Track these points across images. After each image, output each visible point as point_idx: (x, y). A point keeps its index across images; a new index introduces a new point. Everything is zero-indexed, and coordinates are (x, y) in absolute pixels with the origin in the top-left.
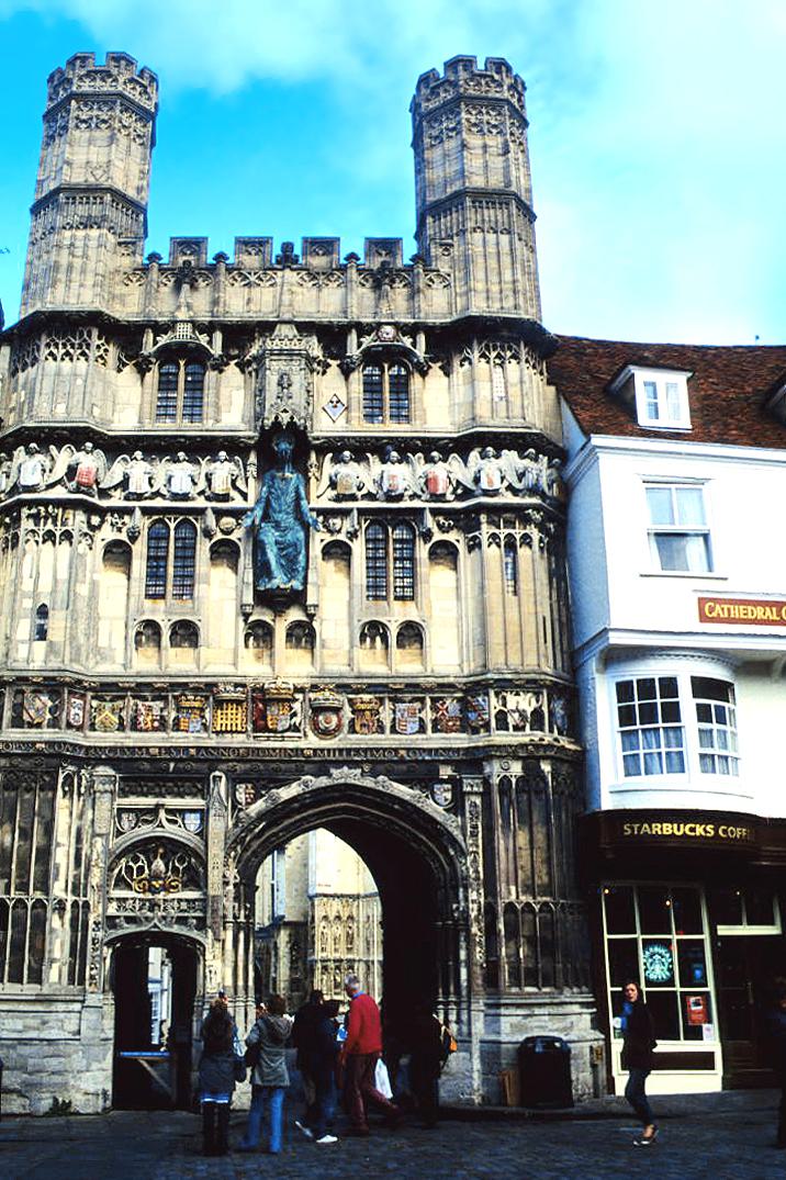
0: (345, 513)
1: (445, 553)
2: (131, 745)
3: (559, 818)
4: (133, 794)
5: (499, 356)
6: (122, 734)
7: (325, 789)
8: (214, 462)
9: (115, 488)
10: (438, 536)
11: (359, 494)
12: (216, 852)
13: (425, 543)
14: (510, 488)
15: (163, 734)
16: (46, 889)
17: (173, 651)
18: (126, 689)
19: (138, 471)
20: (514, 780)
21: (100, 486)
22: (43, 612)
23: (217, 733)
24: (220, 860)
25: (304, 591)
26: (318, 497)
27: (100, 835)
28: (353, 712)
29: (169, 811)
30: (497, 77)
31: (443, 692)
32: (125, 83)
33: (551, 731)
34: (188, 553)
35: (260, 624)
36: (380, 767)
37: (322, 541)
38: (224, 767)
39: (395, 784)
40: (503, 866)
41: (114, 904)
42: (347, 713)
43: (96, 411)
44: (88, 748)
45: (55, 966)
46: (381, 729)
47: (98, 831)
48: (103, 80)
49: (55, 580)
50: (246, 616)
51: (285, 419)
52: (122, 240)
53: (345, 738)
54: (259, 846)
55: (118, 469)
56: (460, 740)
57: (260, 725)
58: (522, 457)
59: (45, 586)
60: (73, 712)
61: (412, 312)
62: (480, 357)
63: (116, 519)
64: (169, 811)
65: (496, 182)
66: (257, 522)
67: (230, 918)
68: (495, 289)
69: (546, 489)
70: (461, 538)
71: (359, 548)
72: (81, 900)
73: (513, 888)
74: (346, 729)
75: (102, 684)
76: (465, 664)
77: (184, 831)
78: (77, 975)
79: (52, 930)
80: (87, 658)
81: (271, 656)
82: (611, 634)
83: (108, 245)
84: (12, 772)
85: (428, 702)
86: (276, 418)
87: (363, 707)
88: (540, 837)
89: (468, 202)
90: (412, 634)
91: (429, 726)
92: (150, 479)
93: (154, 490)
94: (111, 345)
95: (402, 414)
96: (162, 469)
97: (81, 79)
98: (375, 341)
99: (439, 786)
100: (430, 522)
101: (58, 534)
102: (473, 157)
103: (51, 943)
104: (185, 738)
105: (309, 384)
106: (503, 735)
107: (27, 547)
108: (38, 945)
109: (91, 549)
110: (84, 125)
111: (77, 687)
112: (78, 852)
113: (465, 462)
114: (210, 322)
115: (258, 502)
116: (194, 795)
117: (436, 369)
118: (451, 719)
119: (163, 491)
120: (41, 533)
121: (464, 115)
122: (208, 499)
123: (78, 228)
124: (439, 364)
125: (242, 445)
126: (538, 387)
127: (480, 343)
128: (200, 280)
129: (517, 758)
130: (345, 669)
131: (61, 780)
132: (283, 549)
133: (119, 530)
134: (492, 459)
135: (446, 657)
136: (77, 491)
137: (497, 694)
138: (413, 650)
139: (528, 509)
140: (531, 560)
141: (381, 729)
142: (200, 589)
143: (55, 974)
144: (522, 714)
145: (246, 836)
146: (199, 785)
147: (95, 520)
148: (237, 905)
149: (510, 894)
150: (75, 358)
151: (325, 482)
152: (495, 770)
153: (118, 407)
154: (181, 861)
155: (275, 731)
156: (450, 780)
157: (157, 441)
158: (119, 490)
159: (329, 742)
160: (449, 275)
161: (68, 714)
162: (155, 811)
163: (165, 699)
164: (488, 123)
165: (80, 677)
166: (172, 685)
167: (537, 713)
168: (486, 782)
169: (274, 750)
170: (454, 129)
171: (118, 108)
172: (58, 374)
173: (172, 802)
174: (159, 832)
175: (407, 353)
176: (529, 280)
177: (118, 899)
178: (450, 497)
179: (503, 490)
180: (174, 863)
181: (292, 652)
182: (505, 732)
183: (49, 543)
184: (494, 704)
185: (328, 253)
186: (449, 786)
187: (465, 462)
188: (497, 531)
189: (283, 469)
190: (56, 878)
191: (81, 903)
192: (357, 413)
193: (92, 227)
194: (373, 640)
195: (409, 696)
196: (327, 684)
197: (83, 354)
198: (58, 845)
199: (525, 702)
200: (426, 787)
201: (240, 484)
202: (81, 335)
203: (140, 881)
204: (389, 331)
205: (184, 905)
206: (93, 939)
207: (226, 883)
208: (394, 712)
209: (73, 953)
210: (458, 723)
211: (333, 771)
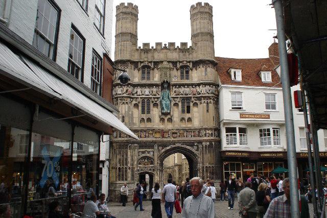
1: (195, 104)
10: (195, 102)
12: (156, 158)
16: (127, 165)
19: (139, 90)
22: (123, 117)
35: (162, 118)
46: (184, 136)
71: (180, 104)
77: (150, 155)
78: (133, 178)
88: (212, 156)
90: (190, 120)
95: (187, 78)
97: (122, 8)
112: (132, 159)
117: (194, 69)
135: (196, 123)
140: (211, 106)
141: (184, 136)
146: (152, 147)
147: (132, 100)
149: (207, 165)
152: (204, 144)
162: (145, 152)
167: (212, 134)
173: (148, 150)
175: (189, 66)
199: (210, 132)
204: (185, 62)
209: (132, 176)
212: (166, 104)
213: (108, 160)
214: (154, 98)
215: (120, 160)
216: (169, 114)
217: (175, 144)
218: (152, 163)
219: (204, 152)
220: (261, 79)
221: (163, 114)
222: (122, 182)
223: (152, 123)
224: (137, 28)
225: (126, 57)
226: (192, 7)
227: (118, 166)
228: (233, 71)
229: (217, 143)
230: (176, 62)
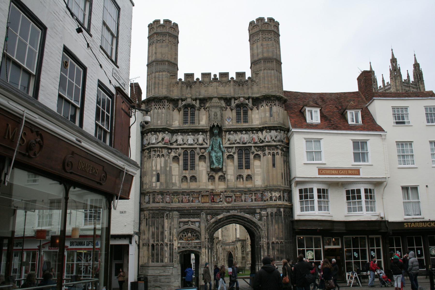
0: (232, 147)
1: (257, 157)
3: (285, 221)
4: (183, 218)
5: (271, 105)
6: (179, 204)
7: (229, 216)
8: (199, 135)
9: (174, 142)
10: (256, 153)
11: (236, 142)
12: (203, 232)
13: (253, 154)
16: (163, 240)
17: (191, 183)
18: (179, 193)
19: (179, 138)
20: (274, 213)
21: (171, 142)
23: (202, 203)
24: (204, 233)
25: (222, 168)
28: (235, 197)
30: (270, 23)
33: (283, 200)
34: (193, 158)
36: (242, 210)
38: (204, 211)
39: (246, 214)
40: (271, 233)
41: (179, 244)
42: (234, 198)
43: (168, 122)
44: (171, 208)
45: (166, 259)
46: (242, 201)
47: (175, 227)
49: (161, 167)
50: (208, 174)
51: (216, 124)
52: (171, 75)
55: (175, 138)
56: (261, 203)
57: (213, 201)
58: (276, 132)
59: (159, 168)
63: (175, 150)
64: (191, 222)
66: (210, 151)
67: (207, 247)
69: (283, 140)
70: (262, 153)
71: (236, 156)
73: (274, 238)
74: (233, 201)
75: (174, 192)
77: (195, 227)
78: (171, 260)
79: (165, 250)
81: (215, 184)
82: (296, 178)
86: (214, 124)
87: (237, 196)
90: (249, 177)
91: (254, 200)
92: (183, 140)
93: (184, 143)
95: (246, 121)
97: (157, 28)
101: (161, 155)
103: (165, 253)
107: (153, 158)
108: (162, 254)
110: (159, 42)
111: (168, 193)
113: (262, 133)
114: (196, 98)
115: (210, 145)
116: (197, 218)
118: (259, 198)
119: (186, 143)
120: (156, 155)
121: (261, 36)
122: (198, 145)
123: (159, 72)
124: (256, 107)
126: (282, 112)
127: (266, 101)
128: (193, 85)
129: (275, 207)
132: (217, 157)
133: (176, 153)
136: (165, 144)
137: (270, 192)
138: (249, 182)
140: (279, 159)
141: (242, 201)
142: (197, 168)
143: (166, 260)
144: (276, 197)
147: (170, 151)
151: (227, 140)
152: (269, 210)
154: (195, 233)
155: (216, 202)
156: (260, 213)
157: (184, 130)
161: (166, 200)
162: (188, 222)
163: (189, 195)
164: (268, 38)
165: (169, 191)
166: (191, 192)
167: (280, 196)
168: (267, 213)
169: (216, 207)
170: (258, 39)
171: (167, 36)
172: (158, 112)
173: (192, 220)
174: (189, 227)
175: (247, 105)
176: (279, 82)
177: (180, 243)
178: (259, 143)
179: (271, 141)
181: (220, 183)
183: (159, 157)
184: (270, 195)
187: (262, 133)
189: (216, 137)
190: (166, 238)
192: (235, 121)
194: (240, 179)
195: (249, 193)
197: (164, 107)
198: (166, 231)
199: (277, 194)
201: (206, 141)
202: (163, 102)
205: (196, 244)
207: (206, 238)
211: (231, 212)
212: (216, 157)
213: (136, 233)
214: (201, 149)
215: (153, 234)
216: (221, 170)
217: (229, 212)
218: (198, 238)
219: (270, 222)
220: (347, 121)
221: (212, 170)
222: (155, 264)
223: (198, 183)
224: (176, 54)
225: (163, 92)
226: (251, 23)
227: (151, 242)
228: (307, 109)
229: (287, 210)
230: (230, 99)
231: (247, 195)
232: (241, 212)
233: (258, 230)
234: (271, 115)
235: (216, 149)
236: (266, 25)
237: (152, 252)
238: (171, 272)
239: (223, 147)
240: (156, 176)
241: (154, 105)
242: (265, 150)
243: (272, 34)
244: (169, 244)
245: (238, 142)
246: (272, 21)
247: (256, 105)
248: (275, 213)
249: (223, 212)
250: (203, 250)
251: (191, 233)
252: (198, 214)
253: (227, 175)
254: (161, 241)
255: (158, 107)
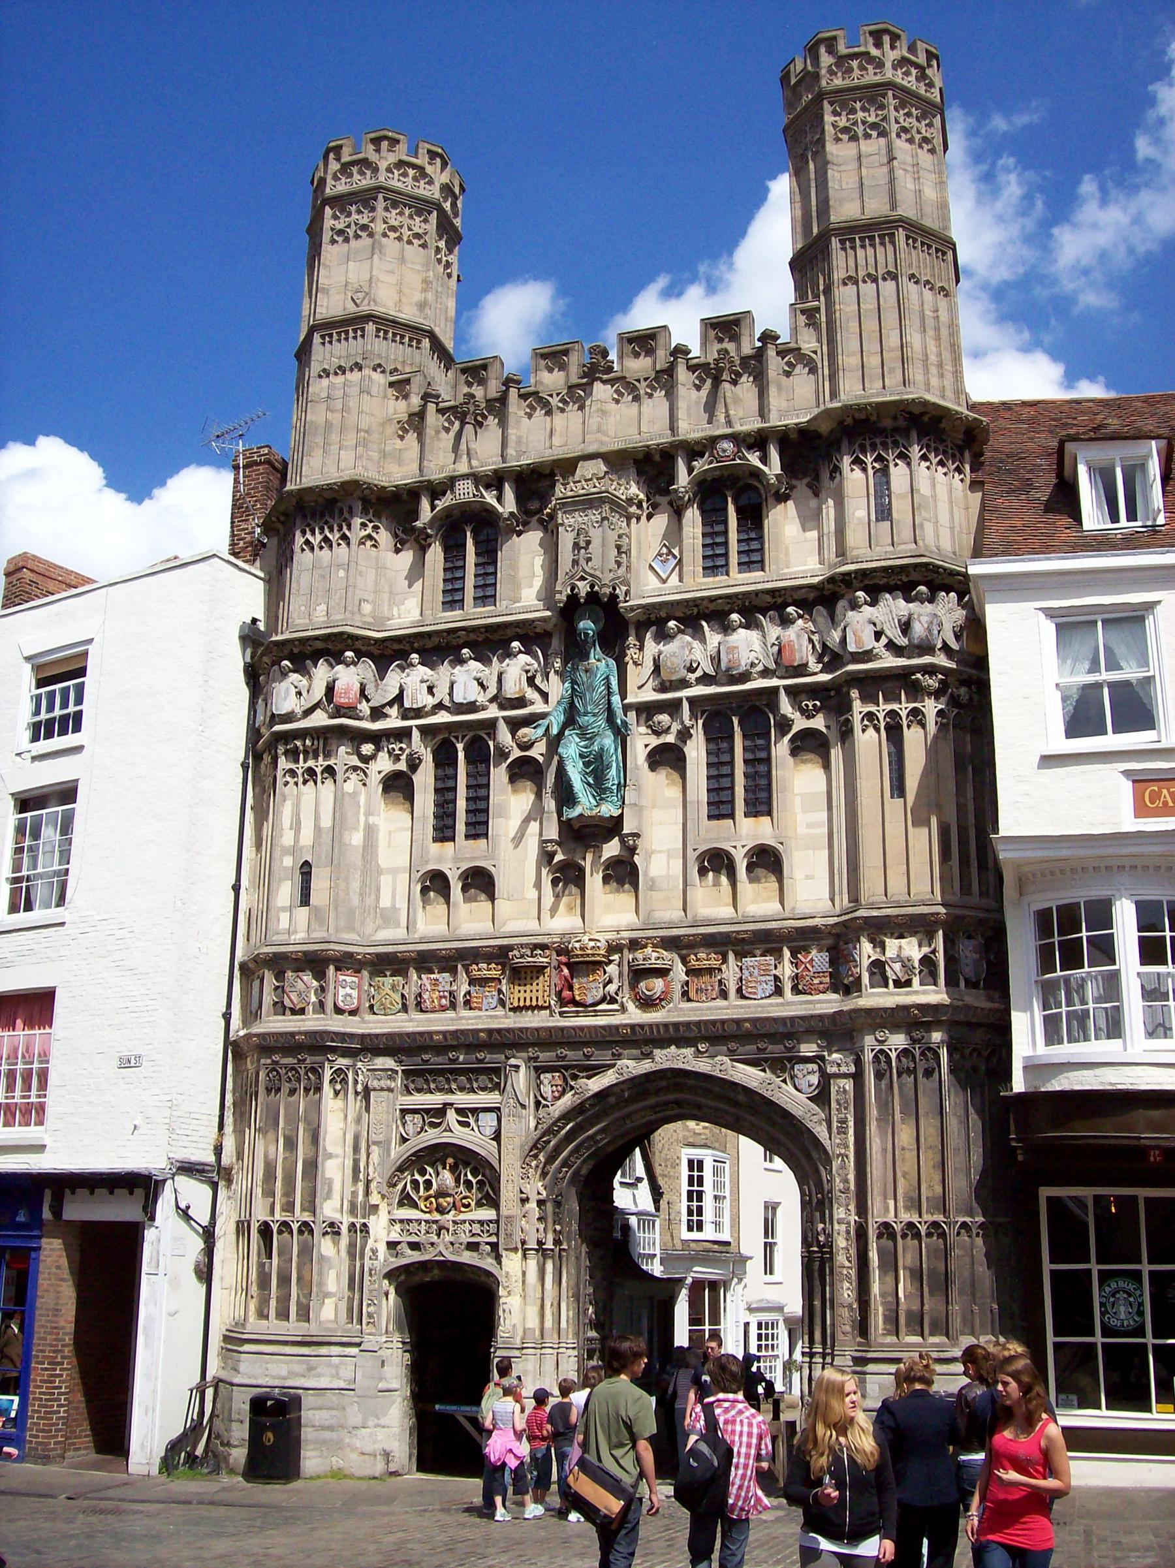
0: (673, 707)
2: (410, 1030)
7: (648, 1076)
9: (390, 704)
10: (800, 723)
14: (891, 646)
15: (450, 1014)
16: (311, 1206)
20: (893, 1055)
22: (306, 870)
23: (512, 1009)
26: (639, 688)
27: (376, 1143)
28: (687, 974)
29: (460, 1112)
30: (874, 52)
31: (805, 939)
32: (389, 170)
37: (646, 746)
43: (367, 608)
44: (363, 1036)
45: (329, 1303)
46: (724, 995)
48: (362, 173)
51: (583, 588)
53: (676, 1009)
54: (571, 1154)
55: (394, 679)
56: (828, 1003)
58: (908, 600)
60: (342, 992)
61: (763, 413)
62: (853, 463)
64: (460, 1112)
65: (876, 207)
66: (555, 731)
68: (873, 361)
71: (696, 751)
72: (359, 1221)
76: (837, 898)
77: (474, 1138)
78: (355, 1313)
79: (322, 1258)
80: (363, 923)
83: (374, 391)
84: (274, 1069)
85: (787, 953)
86: (572, 589)
89: (835, 243)
91: (788, 986)
92: (430, 690)
94: (384, 519)
95: (753, 558)
96: (444, 674)
98: (711, 462)
99: (801, 1066)
100: (786, 707)
102: (843, 175)
103: (320, 1274)
104: (476, 1018)
105: (620, 536)
106: (879, 994)
107: (287, 790)
108: (307, 1277)
109: (364, 785)
111: (347, 962)
112: (356, 1163)
116: (491, 1090)
119: (447, 703)
120: (300, 772)
122: (502, 707)
123: (336, 374)
124: (805, 481)
125: (538, 630)
130: (676, 914)
131: (328, 1074)
133: (397, 759)
134: (866, 608)
139: (914, 674)
141: (724, 995)
144: (906, 963)
145: (549, 1142)
147: (367, 749)
148: (542, 1227)
149: (882, 1210)
150: (335, 545)
151: (649, 666)
153: (398, 598)
156: (819, 1059)
157: (436, 640)
158: (396, 707)
159: (654, 1015)
160: (815, 352)
162: (441, 1112)
163: (453, 971)
164: (864, 123)
167: (928, 962)
169: (582, 1028)
173: (463, 1099)
174: (446, 1138)
175: (756, 474)
176: (938, 338)
177: (401, 1221)
178: (814, 666)
180: (466, 1175)
182: (884, 990)
185: (650, 352)
186: (815, 1067)
187: (832, 616)
188: (873, 709)
189: (586, 657)
190: (329, 1196)
191: (358, 1226)
193: (352, 370)
196: (648, 938)
198: (330, 1156)
199: (912, 949)
200: (783, 1070)
201: (538, 681)
202: (341, 512)
203: (427, 1199)
205: (476, 1228)
206: (371, 1270)
207: (524, 1201)
208: (741, 969)
210: (827, 980)
211: (657, 1052)
213: (189, 1169)
215: (270, 1175)
217: (648, 1056)
219: (873, 1111)
222: (273, 1326)
227: (260, 1214)
231: (748, 961)
232: (712, 1057)
233: (809, 1156)
234: (884, 512)
235: (583, 720)
236: (855, 64)
237: (261, 1266)
238: (347, 1372)
239: (626, 708)
240: (298, 878)
241: (304, 533)
242: (849, 708)
243: (891, 101)
244: (344, 1229)
245: (705, 675)
246: (886, 39)
247: (805, 474)
248: (898, 1056)
249: (619, 1056)
250: (512, 1263)
251: (453, 1169)
252: (497, 1071)
253: (649, 855)
254: (303, 1209)
255: (316, 539)
